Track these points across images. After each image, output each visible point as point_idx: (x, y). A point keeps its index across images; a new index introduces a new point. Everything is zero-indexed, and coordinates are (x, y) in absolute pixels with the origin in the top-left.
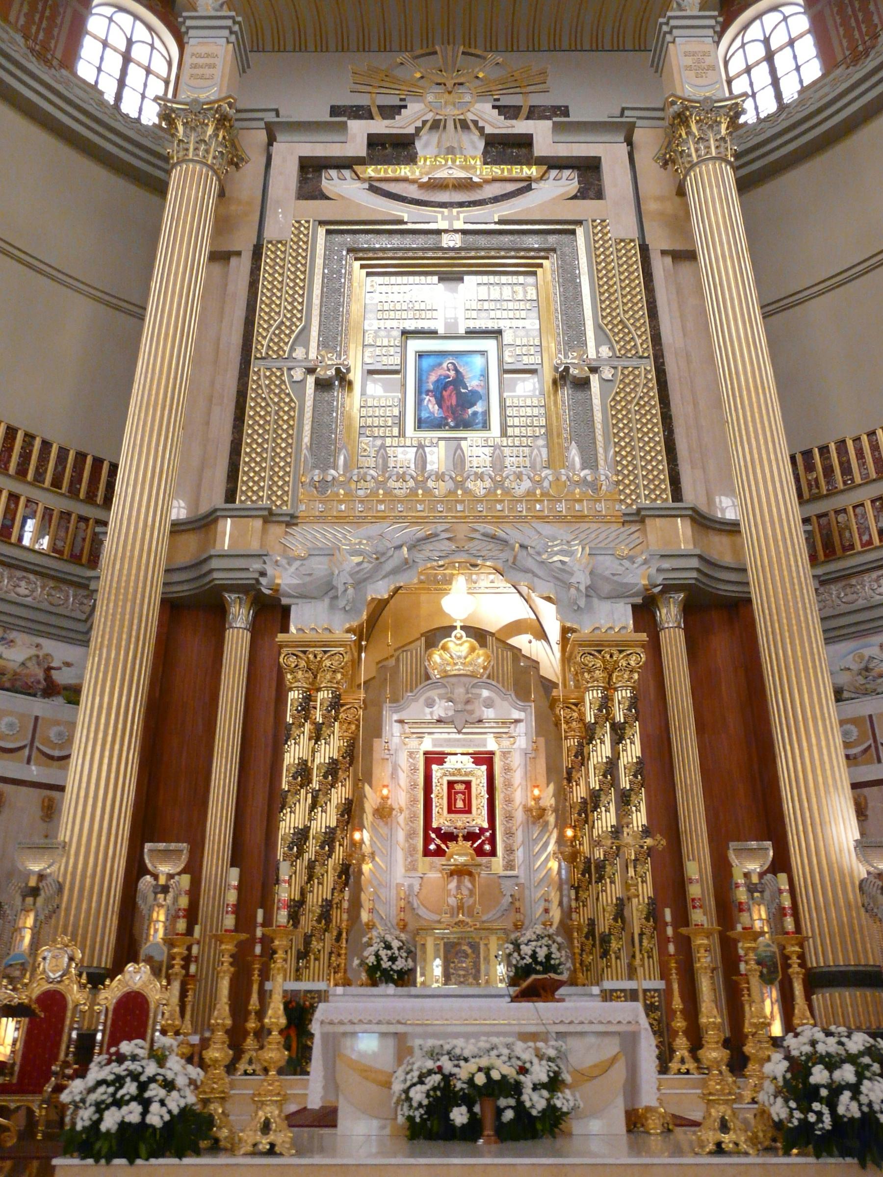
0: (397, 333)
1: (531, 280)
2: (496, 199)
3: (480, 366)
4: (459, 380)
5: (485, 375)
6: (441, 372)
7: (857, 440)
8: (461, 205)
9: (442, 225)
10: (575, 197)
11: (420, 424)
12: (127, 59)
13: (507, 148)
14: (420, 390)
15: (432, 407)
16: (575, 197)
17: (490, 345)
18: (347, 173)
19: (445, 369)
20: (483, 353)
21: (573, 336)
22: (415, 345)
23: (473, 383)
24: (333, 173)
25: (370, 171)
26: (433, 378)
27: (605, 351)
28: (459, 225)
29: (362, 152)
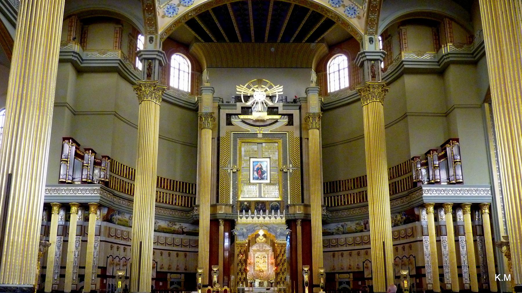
0: (248, 158)
1: (277, 144)
2: (270, 124)
3: (266, 164)
4: (261, 168)
5: (267, 167)
6: (258, 166)
7: (342, 181)
8: (262, 126)
9: (258, 132)
10: (287, 125)
11: (254, 179)
12: (179, 70)
13: (272, 110)
14: (253, 171)
15: (256, 175)
16: (287, 125)
17: (268, 160)
18: (236, 116)
19: (258, 166)
20: (267, 162)
21: (285, 163)
22: (252, 160)
23: (264, 169)
24: (233, 116)
25: (242, 117)
26: (256, 167)
27: (291, 166)
28: (261, 132)
29: (240, 113)
